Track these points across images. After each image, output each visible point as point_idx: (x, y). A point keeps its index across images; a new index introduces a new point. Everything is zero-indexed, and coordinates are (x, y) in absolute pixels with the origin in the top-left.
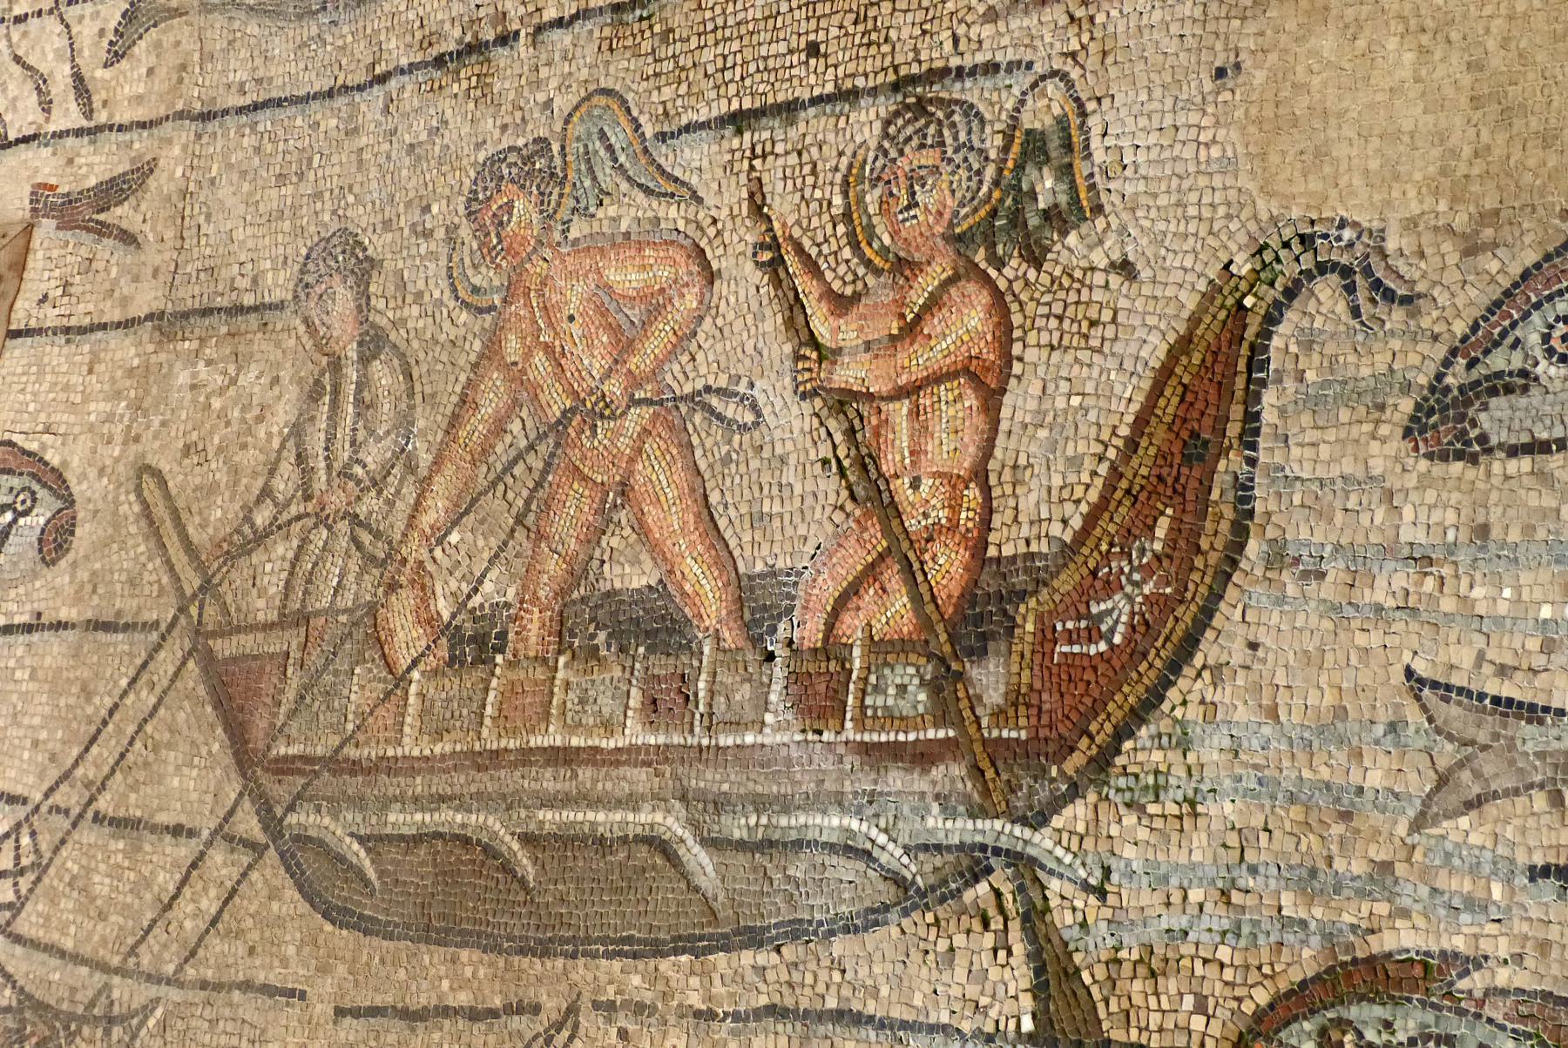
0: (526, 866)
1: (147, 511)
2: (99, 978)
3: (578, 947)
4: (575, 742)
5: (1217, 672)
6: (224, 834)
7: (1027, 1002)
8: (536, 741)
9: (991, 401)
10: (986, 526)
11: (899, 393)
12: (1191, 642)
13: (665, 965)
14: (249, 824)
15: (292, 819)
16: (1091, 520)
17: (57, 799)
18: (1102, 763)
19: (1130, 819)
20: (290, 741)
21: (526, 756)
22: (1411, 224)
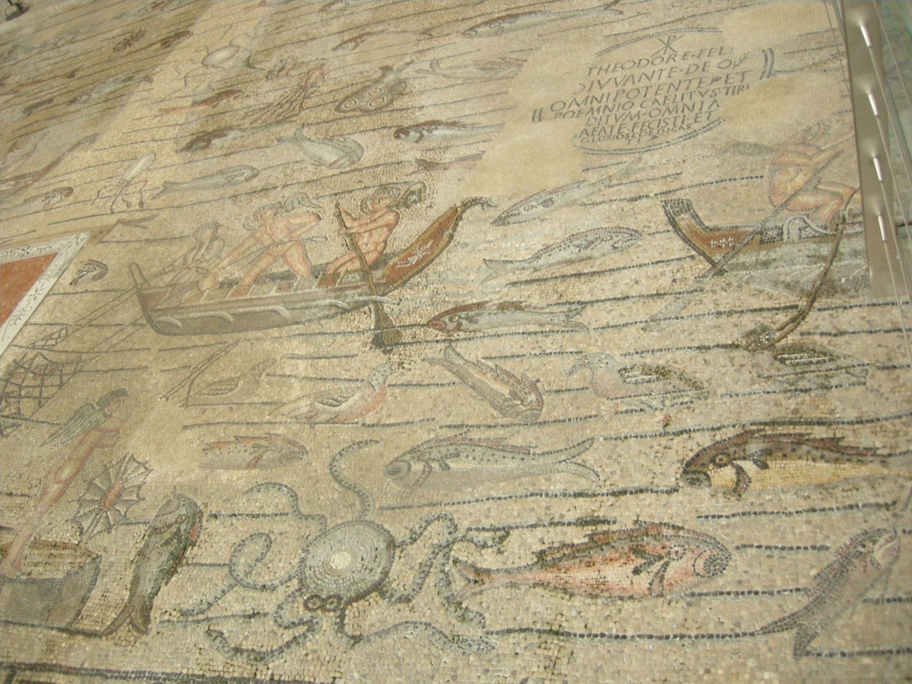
0: (231, 319)
3: (245, 329)
5: (438, 264)
6: (134, 324)
7: (374, 324)
9: (390, 230)
10: (385, 248)
11: (366, 231)
12: (433, 260)
14: (144, 321)
16: (411, 245)
18: (404, 283)
19: (409, 291)
21: (237, 301)
22: (498, 197)
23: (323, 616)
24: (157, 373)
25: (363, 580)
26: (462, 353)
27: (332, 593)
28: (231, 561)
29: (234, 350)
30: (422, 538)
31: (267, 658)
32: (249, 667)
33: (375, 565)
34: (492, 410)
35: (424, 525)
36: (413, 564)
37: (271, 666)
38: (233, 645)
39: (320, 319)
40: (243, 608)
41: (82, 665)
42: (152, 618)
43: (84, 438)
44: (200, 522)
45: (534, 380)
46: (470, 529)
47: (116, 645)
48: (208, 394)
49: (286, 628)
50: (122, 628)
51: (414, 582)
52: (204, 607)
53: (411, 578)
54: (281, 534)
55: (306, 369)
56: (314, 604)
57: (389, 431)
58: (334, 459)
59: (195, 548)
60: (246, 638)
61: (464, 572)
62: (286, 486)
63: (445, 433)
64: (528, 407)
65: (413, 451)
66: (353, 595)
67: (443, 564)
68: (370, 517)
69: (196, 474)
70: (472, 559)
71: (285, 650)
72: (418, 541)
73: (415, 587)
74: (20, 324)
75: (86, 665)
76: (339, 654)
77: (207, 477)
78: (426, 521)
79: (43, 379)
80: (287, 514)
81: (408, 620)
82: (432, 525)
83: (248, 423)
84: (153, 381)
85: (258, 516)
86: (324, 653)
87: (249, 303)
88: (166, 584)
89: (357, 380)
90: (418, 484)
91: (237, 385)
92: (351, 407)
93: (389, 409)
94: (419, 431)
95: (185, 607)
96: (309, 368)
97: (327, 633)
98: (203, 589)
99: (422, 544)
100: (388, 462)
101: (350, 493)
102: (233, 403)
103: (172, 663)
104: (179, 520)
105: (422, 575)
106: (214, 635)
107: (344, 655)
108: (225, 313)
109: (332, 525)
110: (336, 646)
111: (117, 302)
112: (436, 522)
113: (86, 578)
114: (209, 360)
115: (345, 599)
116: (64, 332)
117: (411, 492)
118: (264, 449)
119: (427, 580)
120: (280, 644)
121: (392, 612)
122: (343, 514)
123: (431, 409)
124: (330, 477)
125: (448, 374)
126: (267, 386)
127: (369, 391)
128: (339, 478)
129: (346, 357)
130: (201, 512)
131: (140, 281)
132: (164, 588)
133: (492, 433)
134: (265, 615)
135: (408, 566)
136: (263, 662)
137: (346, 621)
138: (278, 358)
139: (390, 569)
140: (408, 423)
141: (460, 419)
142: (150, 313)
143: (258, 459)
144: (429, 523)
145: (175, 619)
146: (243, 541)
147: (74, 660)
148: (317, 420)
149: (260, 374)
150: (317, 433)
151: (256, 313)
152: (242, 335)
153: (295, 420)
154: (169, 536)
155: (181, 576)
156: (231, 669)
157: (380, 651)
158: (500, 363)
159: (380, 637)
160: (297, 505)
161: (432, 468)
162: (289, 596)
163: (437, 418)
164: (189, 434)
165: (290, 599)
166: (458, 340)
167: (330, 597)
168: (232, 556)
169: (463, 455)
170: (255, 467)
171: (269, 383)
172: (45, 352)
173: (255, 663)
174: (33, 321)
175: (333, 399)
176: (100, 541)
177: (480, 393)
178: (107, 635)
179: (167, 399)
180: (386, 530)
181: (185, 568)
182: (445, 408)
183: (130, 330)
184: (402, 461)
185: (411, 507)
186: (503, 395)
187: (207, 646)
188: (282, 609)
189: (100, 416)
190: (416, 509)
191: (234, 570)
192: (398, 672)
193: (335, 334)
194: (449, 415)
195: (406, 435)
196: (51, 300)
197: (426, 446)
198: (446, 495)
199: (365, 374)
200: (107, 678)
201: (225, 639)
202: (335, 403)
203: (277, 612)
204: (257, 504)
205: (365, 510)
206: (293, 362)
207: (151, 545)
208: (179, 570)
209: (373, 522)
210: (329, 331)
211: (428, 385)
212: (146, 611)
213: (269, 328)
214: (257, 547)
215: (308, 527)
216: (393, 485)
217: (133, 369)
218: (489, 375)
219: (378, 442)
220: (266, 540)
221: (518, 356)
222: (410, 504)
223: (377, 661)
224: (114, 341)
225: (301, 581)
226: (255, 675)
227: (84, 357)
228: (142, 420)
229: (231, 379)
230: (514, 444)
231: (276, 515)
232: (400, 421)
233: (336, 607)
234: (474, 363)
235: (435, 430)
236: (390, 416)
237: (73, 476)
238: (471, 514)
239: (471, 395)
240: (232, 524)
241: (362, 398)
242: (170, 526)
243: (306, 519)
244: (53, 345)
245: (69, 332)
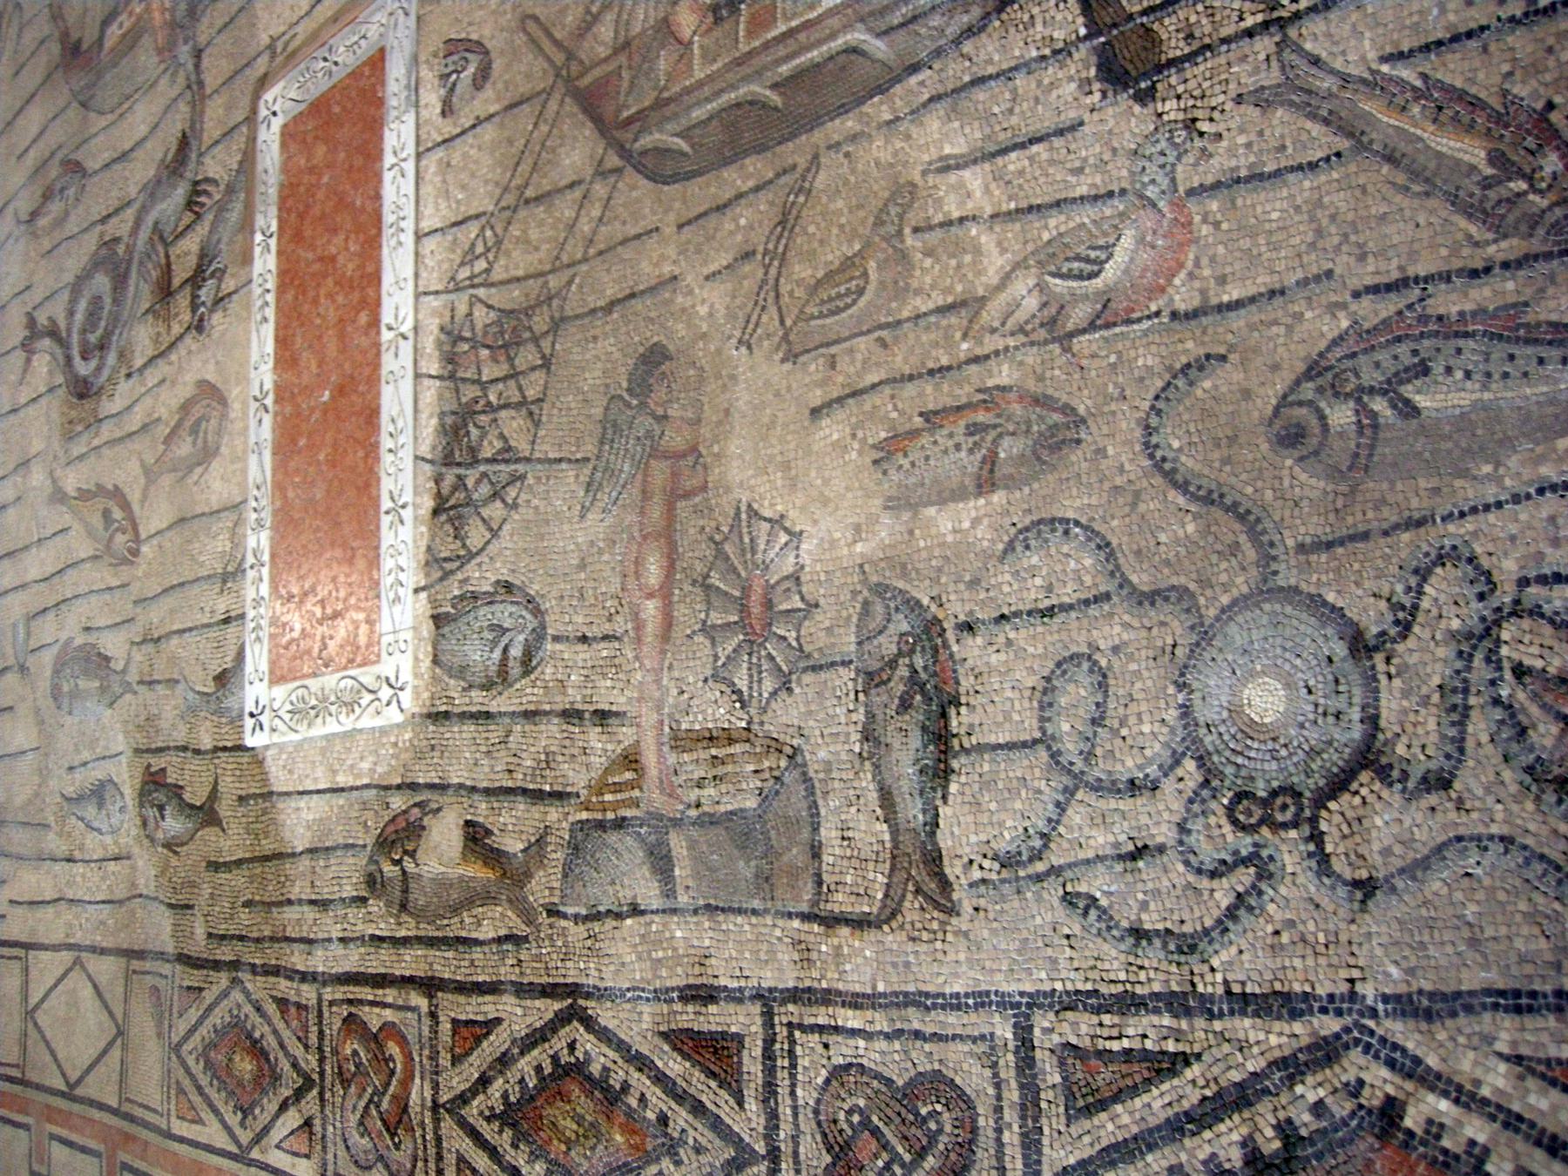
0: (775, 99)
1: (533, 41)
2: (540, 281)
3: (814, 122)
4: (794, 24)
6: (601, 173)
7: (1080, 20)
8: (770, 35)
13: (866, 108)
14: (613, 160)
15: (637, 145)
17: (503, 204)
20: (628, 107)
21: (766, 46)
23: (1277, 841)
24: (701, 287)
25: (1330, 743)
26: (1324, 55)
27: (1275, 784)
28: (1043, 730)
29: (821, 180)
30: (1420, 618)
31: (1202, 946)
32: (1174, 969)
33: (1339, 703)
34: (1463, 223)
35: (1413, 581)
36: (1424, 690)
37: (1215, 962)
38: (1125, 924)
39: (957, 42)
40: (1111, 839)
41: (874, 987)
42: (952, 878)
43: (645, 475)
44: (946, 645)
45: (1539, 105)
46: (1524, 582)
47: (913, 939)
48: (821, 316)
49: (1213, 875)
50: (907, 904)
51: (1443, 737)
52: (1037, 843)
53: (1432, 725)
54: (1116, 649)
55: (987, 190)
56: (1249, 814)
57: (1238, 320)
58: (1149, 430)
59: (963, 710)
60: (1144, 906)
61: (1549, 698)
62: (1077, 523)
63: (1375, 311)
64: (1552, 197)
65: (1314, 370)
66: (1322, 783)
67: (1493, 683)
68: (1287, 576)
69: (887, 529)
70: (1557, 662)
71: (1230, 925)
72: (1416, 629)
73: (1449, 748)
74: (408, 239)
75: (881, 988)
76: (1343, 925)
77: (911, 532)
78: (1416, 571)
79: (510, 360)
80: (1107, 596)
81: (1462, 831)
82: (1433, 580)
83: (931, 372)
84: (703, 310)
85: (1049, 612)
86: (1311, 926)
87: (792, 45)
88: (944, 798)
89: (1111, 194)
90: (1361, 463)
91: (865, 274)
92: (1126, 271)
93: (1213, 260)
94: (1309, 315)
95: (1002, 846)
96: (993, 186)
97: (1301, 880)
98: (1018, 805)
99: (1426, 635)
100: (1269, 410)
101: (1217, 513)
102: (881, 327)
103: (1029, 971)
104: (905, 648)
105: (1455, 717)
106: (1081, 905)
107: (1353, 927)
108: (755, 88)
109: (1212, 612)
110: (1330, 908)
111: (544, 128)
112: (1439, 570)
113: (796, 801)
114: (782, 223)
115: (1308, 794)
116: (489, 233)
117: (1353, 490)
118: (992, 434)
119: (1470, 729)
120: (1216, 913)
121: (1419, 818)
122: (1224, 578)
123: (1313, 245)
124: (1158, 480)
125: (1316, 129)
126: (928, 262)
127: (1148, 220)
128: (1179, 478)
129: (1060, 132)
130: (936, 621)
131: (559, 58)
132: (943, 811)
133: (1487, 292)
134: (1161, 849)
135: (1415, 699)
136: (1196, 956)
137: (1329, 848)
138: (917, 178)
139: (1377, 708)
140: (1272, 293)
141: (1395, 263)
142: (617, 134)
143: (991, 460)
144: (1423, 574)
145: (994, 876)
146: (1048, 679)
147: (857, 979)
148: (1070, 326)
149: (900, 233)
150: (1084, 362)
151: (816, 67)
152: (818, 136)
153: (1022, 338)
154: (902, 687)
155: (963, 779)
156: (1142, 976)
157: (1424, 912)
158: (1428, 64)
159: (1414, 878)
160: (1118, 567)
161: (1374, 415)
162: (1191, 801)
163: (1338, 271)
164: (832, 429)
165: (1196, 807)
166: (1297, 16)
167: (1274, 793)
168: (1042, 719)
169: (1438, 368)
170: (993, 487)
171: (928, 253)
172: (481, 292)
173: (1183, 959)
174: (426, 225)
175: (1078, 258)
176: (785, 716)
177: (1415, 175)
178: (887, 921)
179: (749, 347)
180: (1333, 608)
181: (963, 759)
182: (1346, 236)
183: (600, 189)
184: (1300, 404)
185: (1365, 536)
186: (1473, 168)
187: (1077, 929)
188: (1189, 832)
189: (644, 423)
190: (1382, 541)
191: (1059, 753)
192: (1479, 959)
193: (1006, 75)
194: (1362, 258)
195: (1282, 330)
196: (431, 162)
197: (1338, 352)
198: (1436, 491)
199: (1121, 173)
200: (927, 1009)
201: (1105, 912)
202: (1088, 268)
203: (1181, 843)
204: (1038, 581)
205: (1267, 559)
206: (952, 177)
207: (879, 712)
208: (955, 764)
209: (1296, 590)
210: (991, 70)
211: (1277, 173)
212: (934, 860)
213: (861, 101)
214: (1077, 693)
215: (1163, 624)
216: (1303, 477)
217: (652, 290)
218: (1416, 110)
219: (1223, 358)
220: (1091, 671)
221: (1470, 35)
222: (1361, 528)
223: (1426, 938)
224: (585, 227)
225: (1200, 760)
226: (1193, 985)
227: (554, 282)
228: (727, 412)
229: (848, 263)
230: (1554, 317)
231: (1087, 602)
232: (1251, 290)
233: (1297, 815)
234: (1363, 81)
235: (1343, 306)
236: (1222, 280)
237: (670, 569)
238: (1513, 538)
239: (1394, 184)
240: (1009, 642)
241: (1141, 241)
242: (892, 664)
243: (1153, 604)
244: (487, 271)
245: (499, 230)
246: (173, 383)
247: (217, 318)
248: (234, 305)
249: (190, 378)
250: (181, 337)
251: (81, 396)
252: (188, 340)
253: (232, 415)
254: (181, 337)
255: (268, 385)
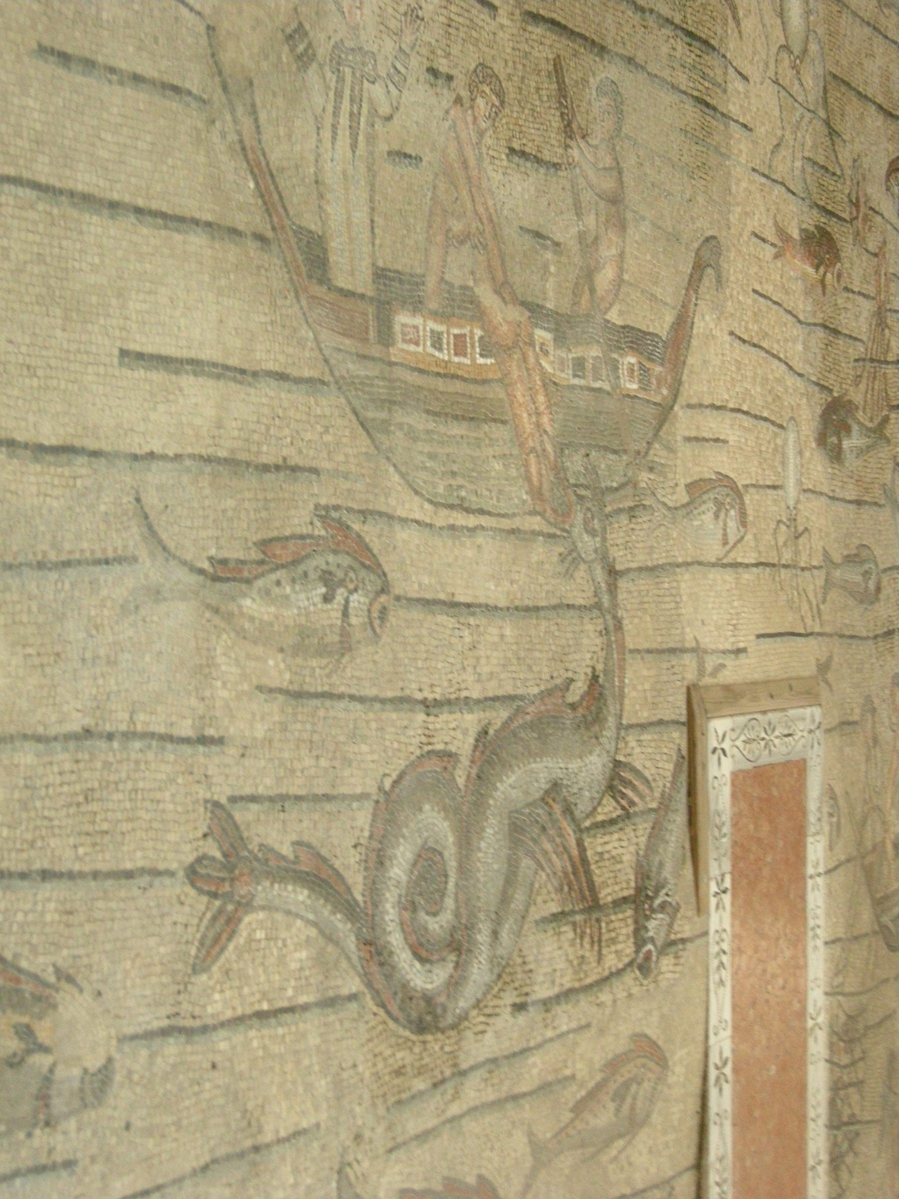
246: (602, 1032)
247: (666, 963)
248: (689, 953)
249: (625, 1029)
250: (619, 972)
251: (421, 1028)
252: (629, 978)
253: (672, 1079)
254: (619, 972)
255: (727, 1053)
